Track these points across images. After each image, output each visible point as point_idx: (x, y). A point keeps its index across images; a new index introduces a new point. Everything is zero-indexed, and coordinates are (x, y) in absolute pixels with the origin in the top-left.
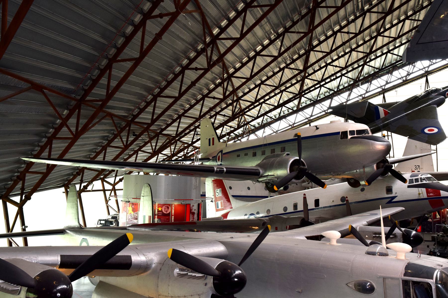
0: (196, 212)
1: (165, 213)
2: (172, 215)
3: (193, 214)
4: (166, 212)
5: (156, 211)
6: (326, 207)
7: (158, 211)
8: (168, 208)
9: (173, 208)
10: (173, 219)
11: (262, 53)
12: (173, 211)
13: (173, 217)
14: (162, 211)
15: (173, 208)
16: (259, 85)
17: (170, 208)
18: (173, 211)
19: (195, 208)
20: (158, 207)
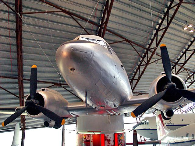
0: (112, 140)
1: (87, 139)
2: (91, 141)
3: (109, 141)
4: (88, 139)
5: (83, 138)
6: (125, 140)
7: (84, 139)
8: (89, 136)
9: (92, 136)
10: (92, 144)
11: (160, 29)
12: (92, 139)
13: (92, 142)
14: (85, 139)
15: (92, 136)
16: (185, 52)
17: (90, 137)
18: (92, 139)
19: (111, 137)
20: (84, 136)
